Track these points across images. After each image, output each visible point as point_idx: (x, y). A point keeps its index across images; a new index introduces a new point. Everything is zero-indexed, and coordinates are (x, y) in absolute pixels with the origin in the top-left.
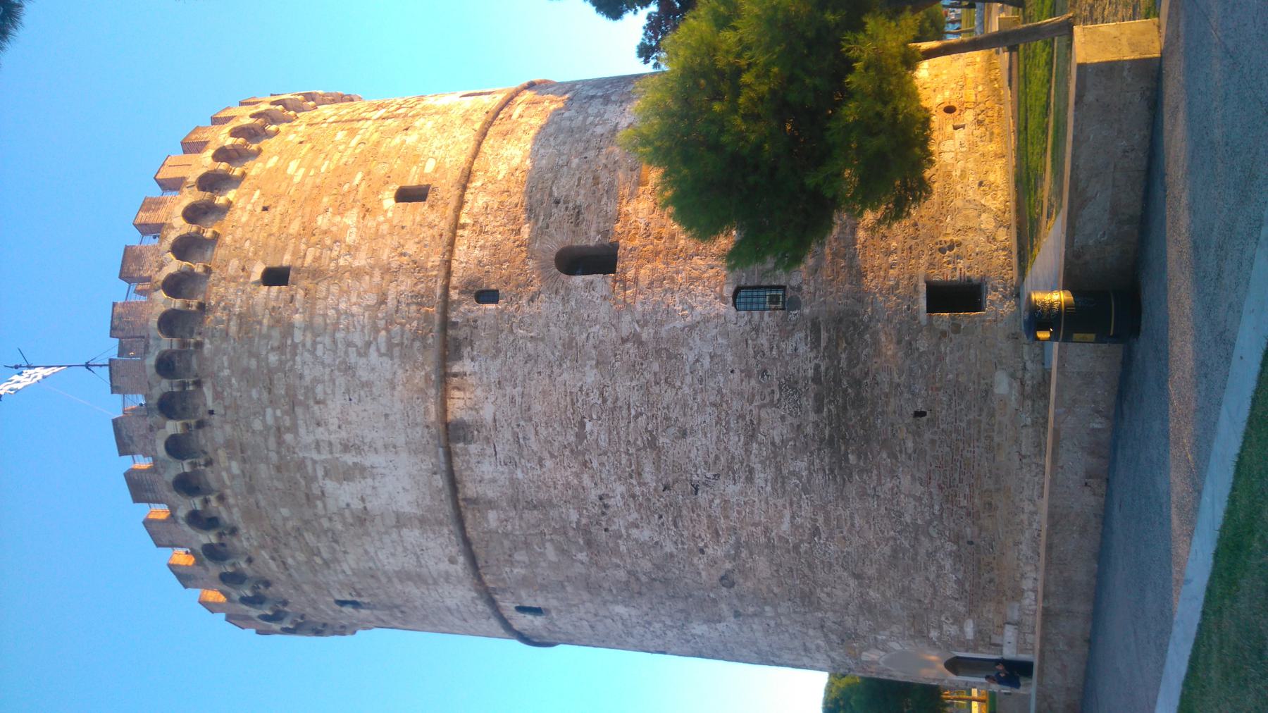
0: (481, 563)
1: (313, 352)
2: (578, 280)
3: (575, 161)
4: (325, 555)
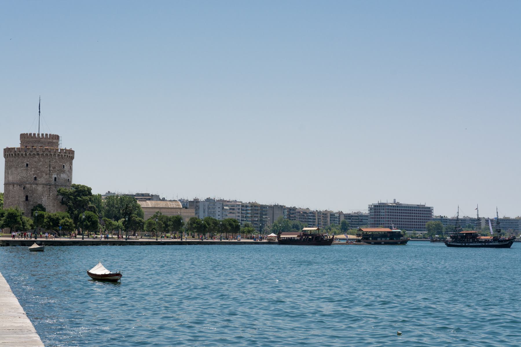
1: (20, 170)
2: (25, 197)
3: (38, 196)
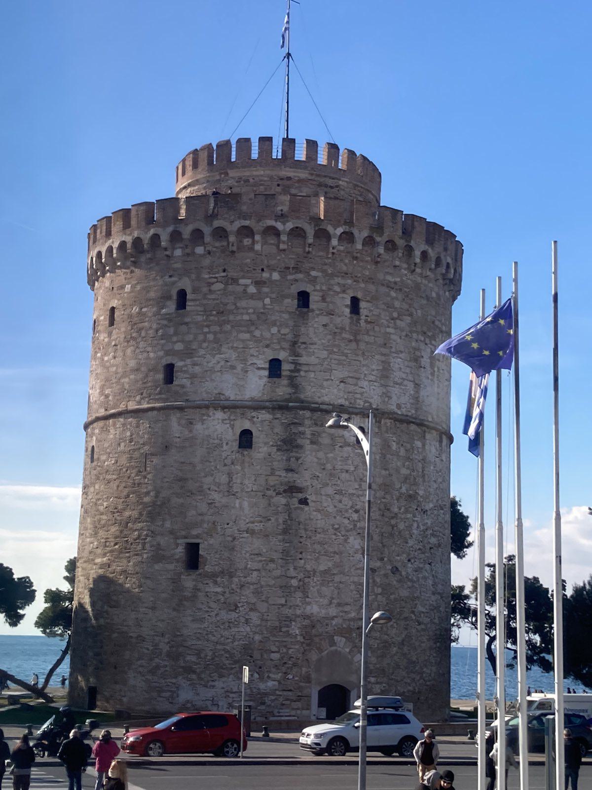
0: (398, 424)
4: (398, 322)
